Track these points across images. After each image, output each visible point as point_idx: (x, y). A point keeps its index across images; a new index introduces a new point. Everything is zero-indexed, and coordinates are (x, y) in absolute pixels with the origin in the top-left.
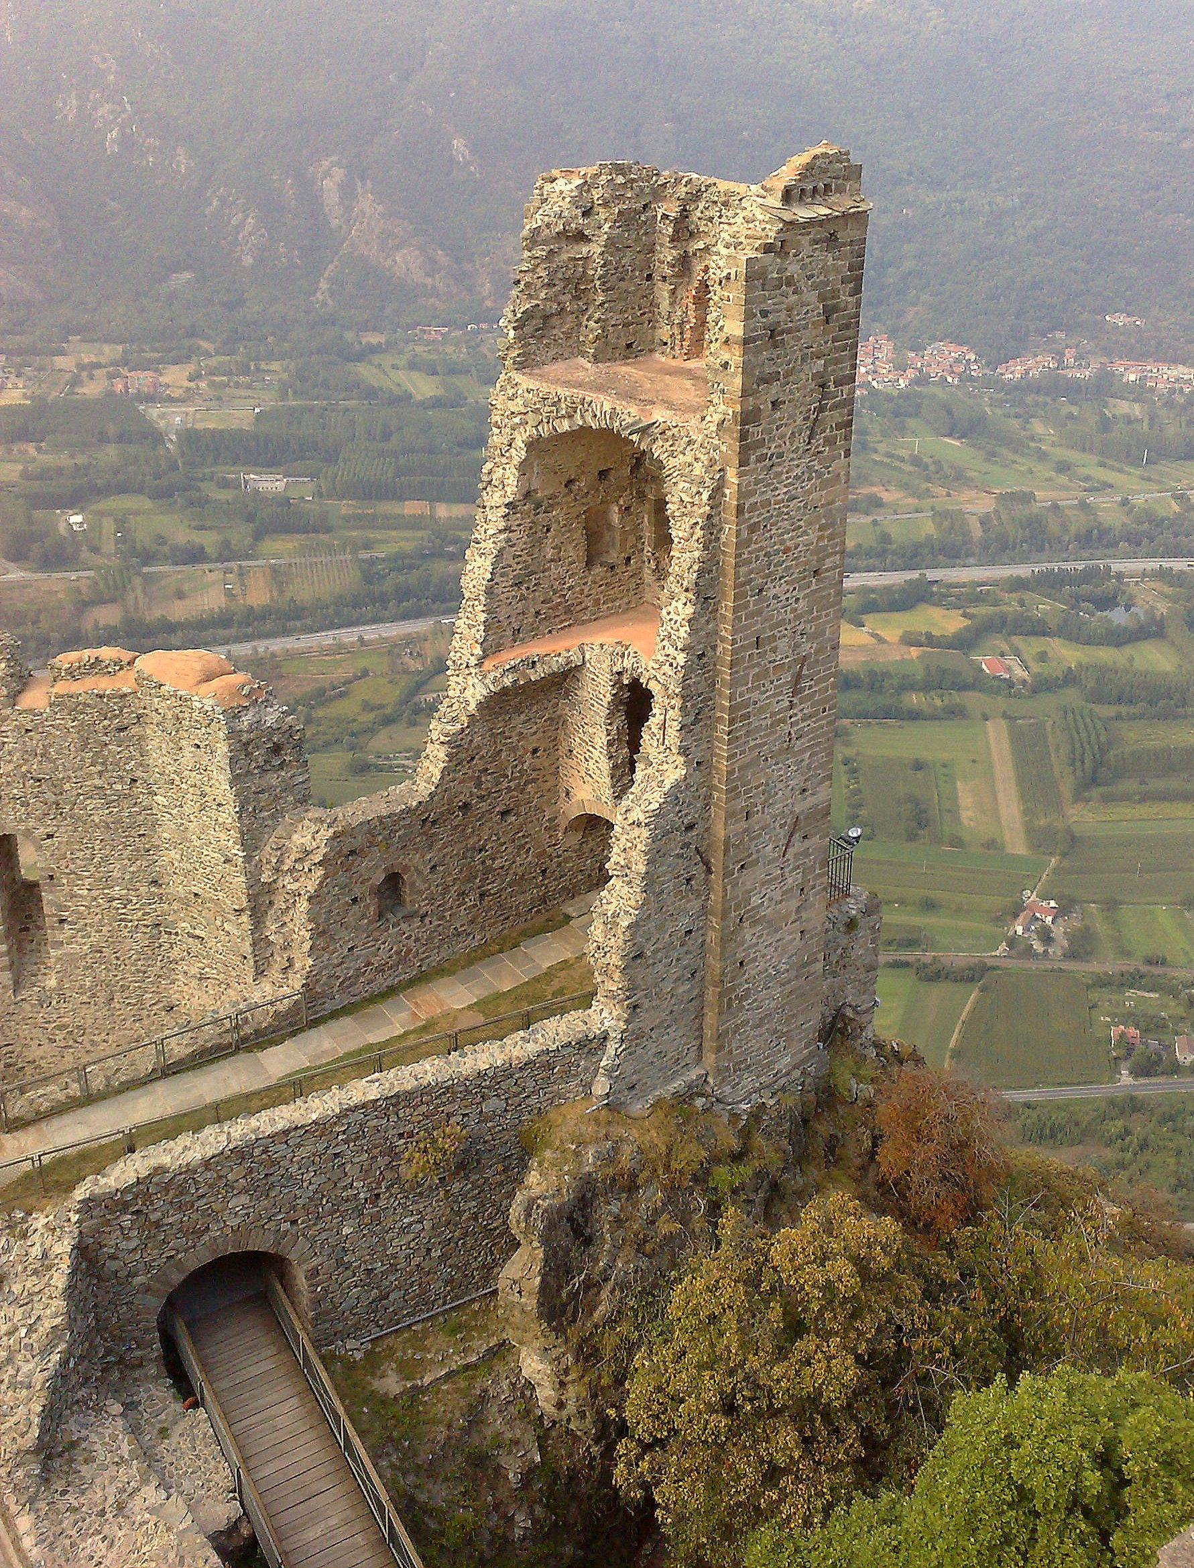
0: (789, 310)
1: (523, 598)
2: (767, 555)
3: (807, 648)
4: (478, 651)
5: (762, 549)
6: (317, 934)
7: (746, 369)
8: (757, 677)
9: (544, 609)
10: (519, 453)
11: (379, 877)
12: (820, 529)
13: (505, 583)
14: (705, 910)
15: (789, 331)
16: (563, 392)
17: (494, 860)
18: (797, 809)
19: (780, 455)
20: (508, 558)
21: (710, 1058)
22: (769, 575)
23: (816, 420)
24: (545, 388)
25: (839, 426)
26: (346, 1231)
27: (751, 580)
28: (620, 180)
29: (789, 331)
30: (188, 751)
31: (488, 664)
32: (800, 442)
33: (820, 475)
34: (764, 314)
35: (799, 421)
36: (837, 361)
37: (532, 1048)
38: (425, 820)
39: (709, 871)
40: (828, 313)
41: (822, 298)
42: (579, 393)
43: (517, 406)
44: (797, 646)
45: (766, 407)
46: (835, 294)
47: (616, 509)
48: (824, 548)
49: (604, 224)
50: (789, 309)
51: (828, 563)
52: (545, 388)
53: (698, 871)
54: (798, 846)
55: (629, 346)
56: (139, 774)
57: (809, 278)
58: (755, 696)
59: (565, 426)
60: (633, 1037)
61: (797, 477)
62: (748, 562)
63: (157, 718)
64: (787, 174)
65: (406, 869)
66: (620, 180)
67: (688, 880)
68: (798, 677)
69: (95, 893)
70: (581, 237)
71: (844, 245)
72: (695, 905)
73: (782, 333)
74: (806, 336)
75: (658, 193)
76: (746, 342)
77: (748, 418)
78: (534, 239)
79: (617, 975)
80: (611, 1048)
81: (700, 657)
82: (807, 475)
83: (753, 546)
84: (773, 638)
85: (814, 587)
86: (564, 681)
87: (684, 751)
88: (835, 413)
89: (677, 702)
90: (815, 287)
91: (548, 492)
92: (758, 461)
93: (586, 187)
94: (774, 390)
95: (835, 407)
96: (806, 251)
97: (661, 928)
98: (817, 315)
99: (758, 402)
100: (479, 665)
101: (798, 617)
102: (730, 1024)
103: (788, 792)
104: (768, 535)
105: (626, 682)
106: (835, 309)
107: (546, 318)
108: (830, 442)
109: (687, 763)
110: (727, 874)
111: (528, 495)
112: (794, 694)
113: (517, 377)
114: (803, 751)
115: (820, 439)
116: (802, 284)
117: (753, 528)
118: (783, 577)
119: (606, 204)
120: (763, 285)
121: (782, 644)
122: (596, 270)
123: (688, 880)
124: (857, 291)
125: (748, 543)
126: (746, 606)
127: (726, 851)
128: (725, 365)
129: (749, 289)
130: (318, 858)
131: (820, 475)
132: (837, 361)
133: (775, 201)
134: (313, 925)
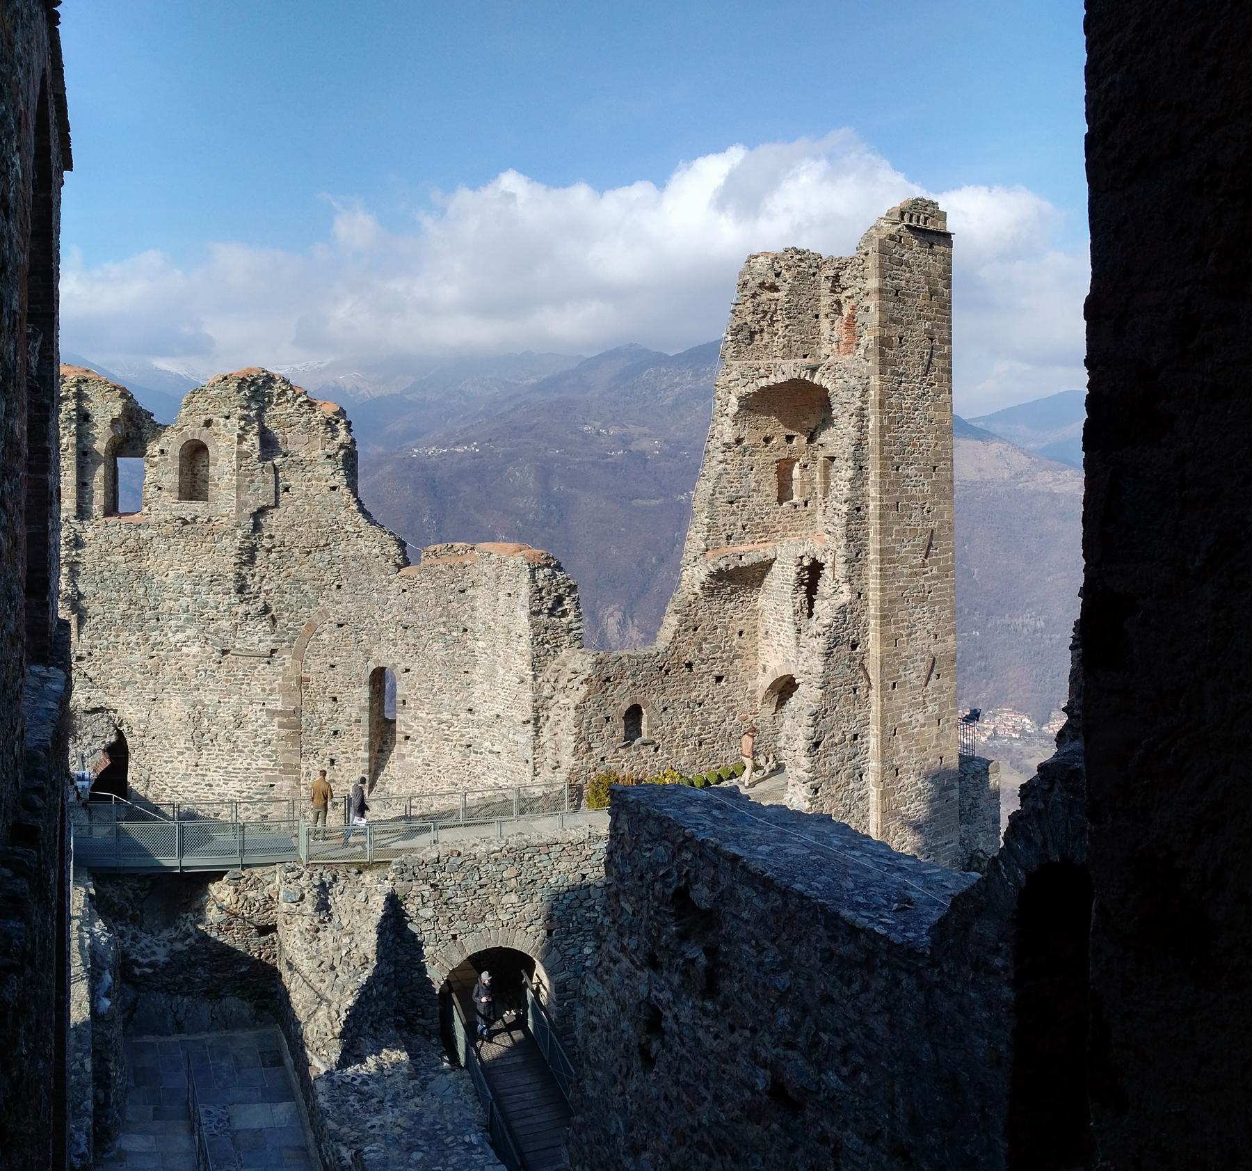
3: (934, 524)
4: (703, 546)
6: (580, 739)
10: (733, 408)
12: (937, 438)
17: (710, 714)
20: (724, 482)
23: (930, 362)
25: (943, 370)
26: (587, 951)
30: (502, 596)
31: (709, 554)
56: (469, 625)
59: (763, 383)
63: (485, 579)
69: (430, 717)
74: (920, 302)
76: (881, 291)
86: (765, 567)
88: (941, 361)
95: (940, 356)
103: (925, 634)
105: (806, 563)
111: (739, 441)
114: (934, 604)
115: (932, 376)
134: (576, 730)
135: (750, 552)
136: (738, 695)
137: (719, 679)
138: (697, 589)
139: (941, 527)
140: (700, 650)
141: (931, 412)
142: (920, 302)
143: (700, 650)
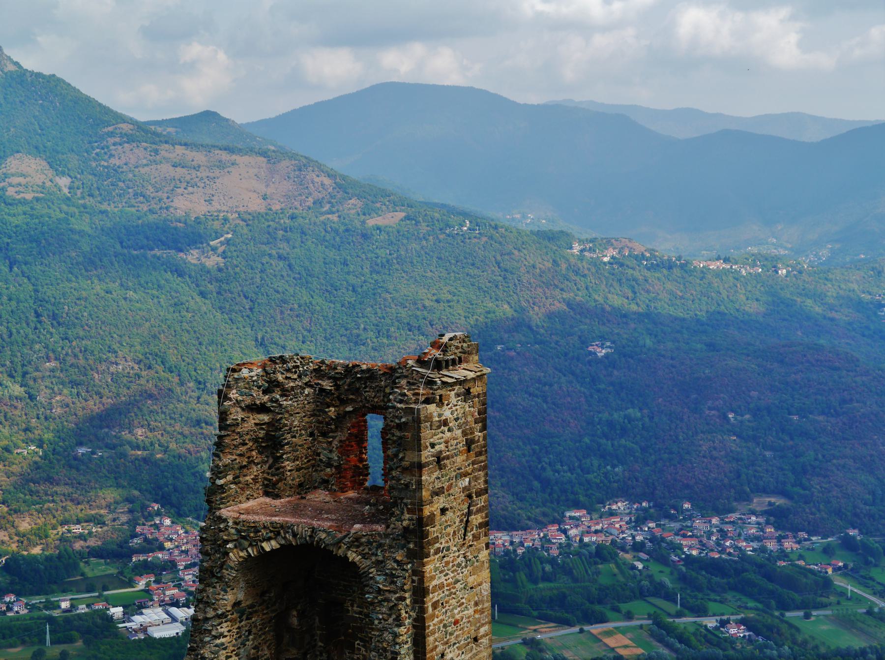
0: (446, 442)
2: (445, 626)
5: (441, 621)
12: (476, 604)
15: (448, 458)
19: (448, 549)
22: (447, 643)
23: (467, 521)
25: (481, 526)
27: (436, 647)
29: (448, 458)
36: (476, 479)
40: (469, 443)
41: (464, 433)
47: (295, 613)
48: (479, 620)
50: (446, 442)
51: (482, 631)
57: (456, 419)
61: (459, 565)
71: (475, 397)
73: (444, 459)
74: (459, 459)
82: (463, 564)
83: (436, 620)
85: (474, 651)
88: (479, 516)
90: (460, 427)
91: (248, 603)
92: (436, 553)
94: (442, 499)
95: (479, 511)
96: (454, 400)
98: (462, 447)
99: (433, 509)
104: (444, 610)
107: (242, 467)
111: (237, 604)
115: (470, 536)
118: (455, 644)
120: (431, 426)
141: (471, 580)
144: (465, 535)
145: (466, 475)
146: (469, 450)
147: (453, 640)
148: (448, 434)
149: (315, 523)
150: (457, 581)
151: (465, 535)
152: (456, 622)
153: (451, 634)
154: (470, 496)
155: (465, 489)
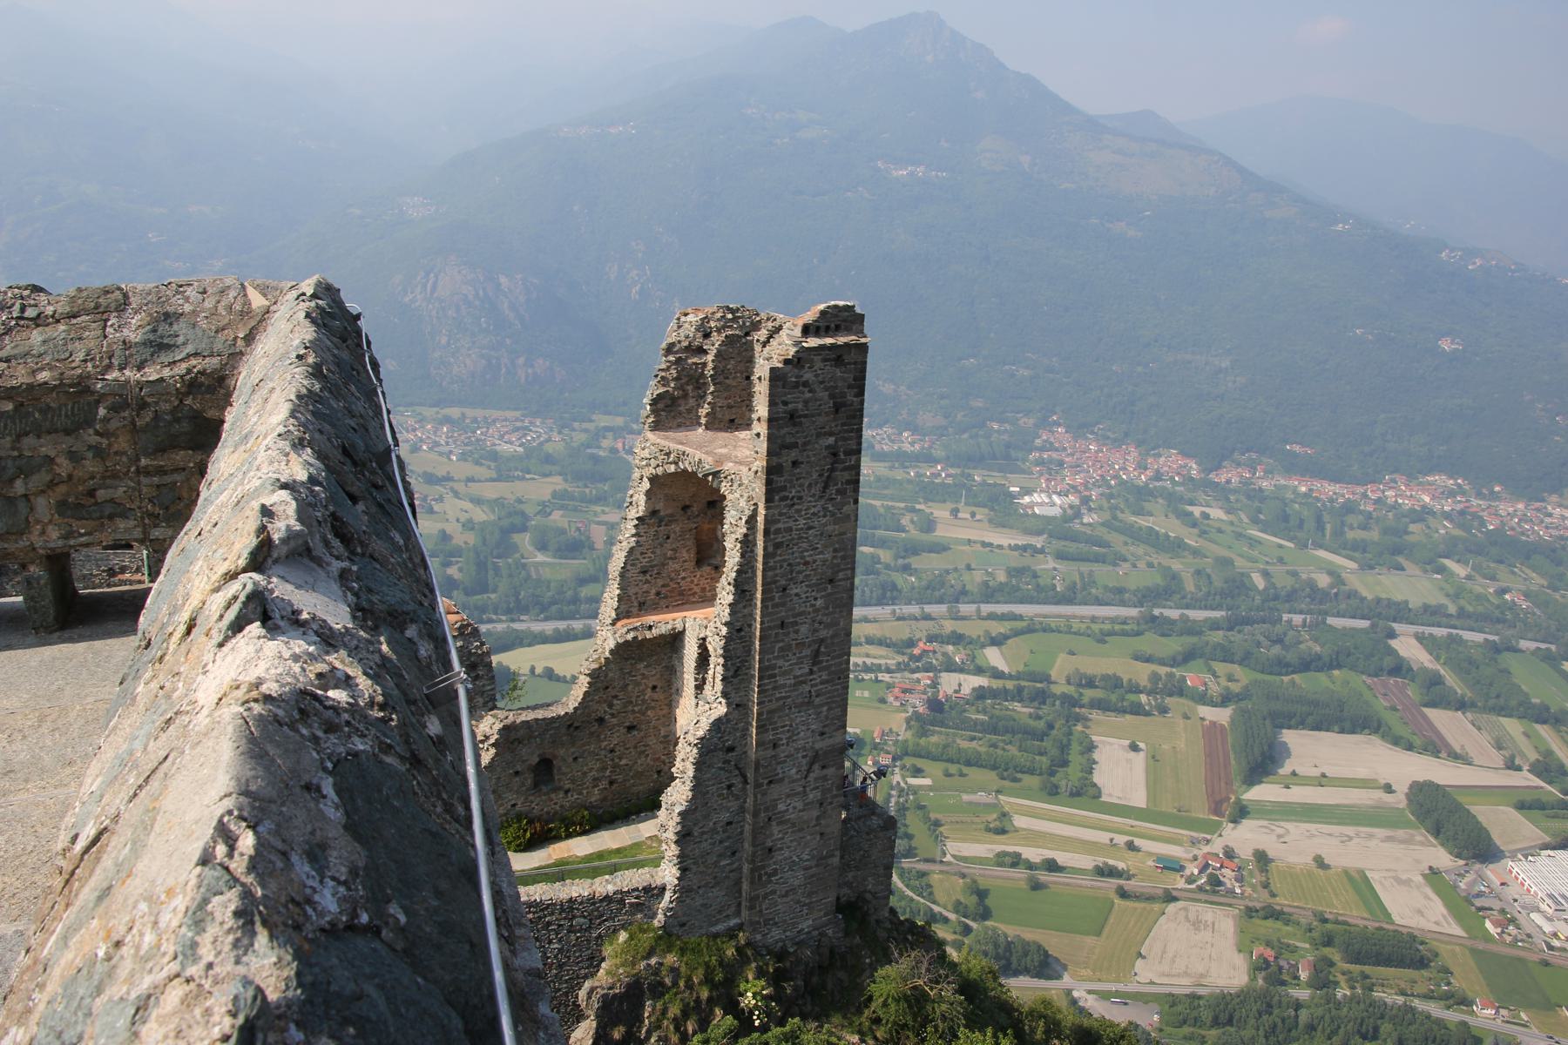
0: (806, 402)
1: (647, 582)
3: (823, 633)
4: (614, 615)
7: (770, 438)
8: (782, 649)
9: (664, 591)
10: (646, 485)
11: (535, 760)
12: (835, 551)
13: (633, 571)
14: (742, 810)
15: (806, 416)
16: (673, 446)
18: (818, 746)
19: (800, 498)
21: (745, 913)
24: (663, 442)
25: (848, 482)
28: (730, 316)
29: (806, 416)
31: (619, 624)
32: (816, 490)
33: (833, 515)
34: (785, 403)
35: (815, 476)
36: (845, 439)
37: (611, 889)
38: (571, 725)
39: (746, 782)
41: (832, 396)
42: (681, 447)
43: (646, 454)
44: (816, 631)
45: (787, 465)
46: (843, 395)
49: (715, 343)
50: (806, 402)
51: (841, 575)
52: (663, 442)
53: (737, 781)
54: (817, 771)
55: (732, 421)
58: (780, 662)
59: (672, 469)
60: (684, 889)
62: (774, 568)
64: (810, 316)
65: (555, 757)
66: (730, 316)
67: (729, 787)
68: (817, 653)
70: (701, 351)
72: (734, 805)
74: (821, 420)
75: (756, 326)
77: (772, 471)
78: (669, 350)
79: (673, 846)
80: (668, 895)
81: (739, 630)
84: (796, 623)
87: (725, 694)
89: (721, 661)
91: (669, 511)
92: (782, 499)
93: (706, 319)
94: (794, 454)
95: (845, 469)
97: (706, 817)
100: (613, 624)
101: (817, 611)
102: (761, 892)
106: (844, 405)
107: (674, 400)
108: (839, 492)
109: (728, 705)
110: (758, 785)
112: (814, 664)
113: (650, 435)
114: (822, 705)
115: (833, 490)
116: (815, 386)
117: (777, 546)
119: (718, 331)
121: (804, 629)
122: (709, 372)
123: (729, 787)
124: (861, 393)
125: (773, 555)
126: (772, 599)
127: (757, 769)
128: (758, 435)
129: (772, 387)
130: (492, 741)
131: (833, 515)
132: (845, 439)
133: (798, 332)
135: (663, 622)
136: (652, 741)
137: (630, 728)
138: (607, 654)
139: (833, 637)
140: (611, 706)
141: (830, 528)
142: (821, 420)
143: (611, 706)
144: (826, 487)
145: (831, 434)
146: (837, 411)
147: (801, 577)
148: (808, 395)
149: (703, 457)
150: (810, 528)
151: (826, 487)
152: (806, 563)
153: (800, 572)
154: (835, 455)
155: (827, 447)
